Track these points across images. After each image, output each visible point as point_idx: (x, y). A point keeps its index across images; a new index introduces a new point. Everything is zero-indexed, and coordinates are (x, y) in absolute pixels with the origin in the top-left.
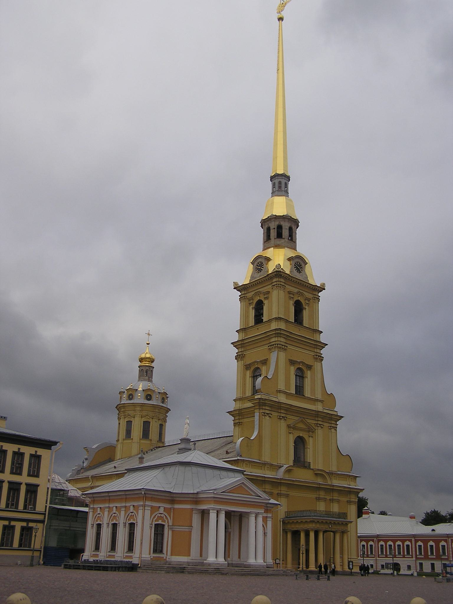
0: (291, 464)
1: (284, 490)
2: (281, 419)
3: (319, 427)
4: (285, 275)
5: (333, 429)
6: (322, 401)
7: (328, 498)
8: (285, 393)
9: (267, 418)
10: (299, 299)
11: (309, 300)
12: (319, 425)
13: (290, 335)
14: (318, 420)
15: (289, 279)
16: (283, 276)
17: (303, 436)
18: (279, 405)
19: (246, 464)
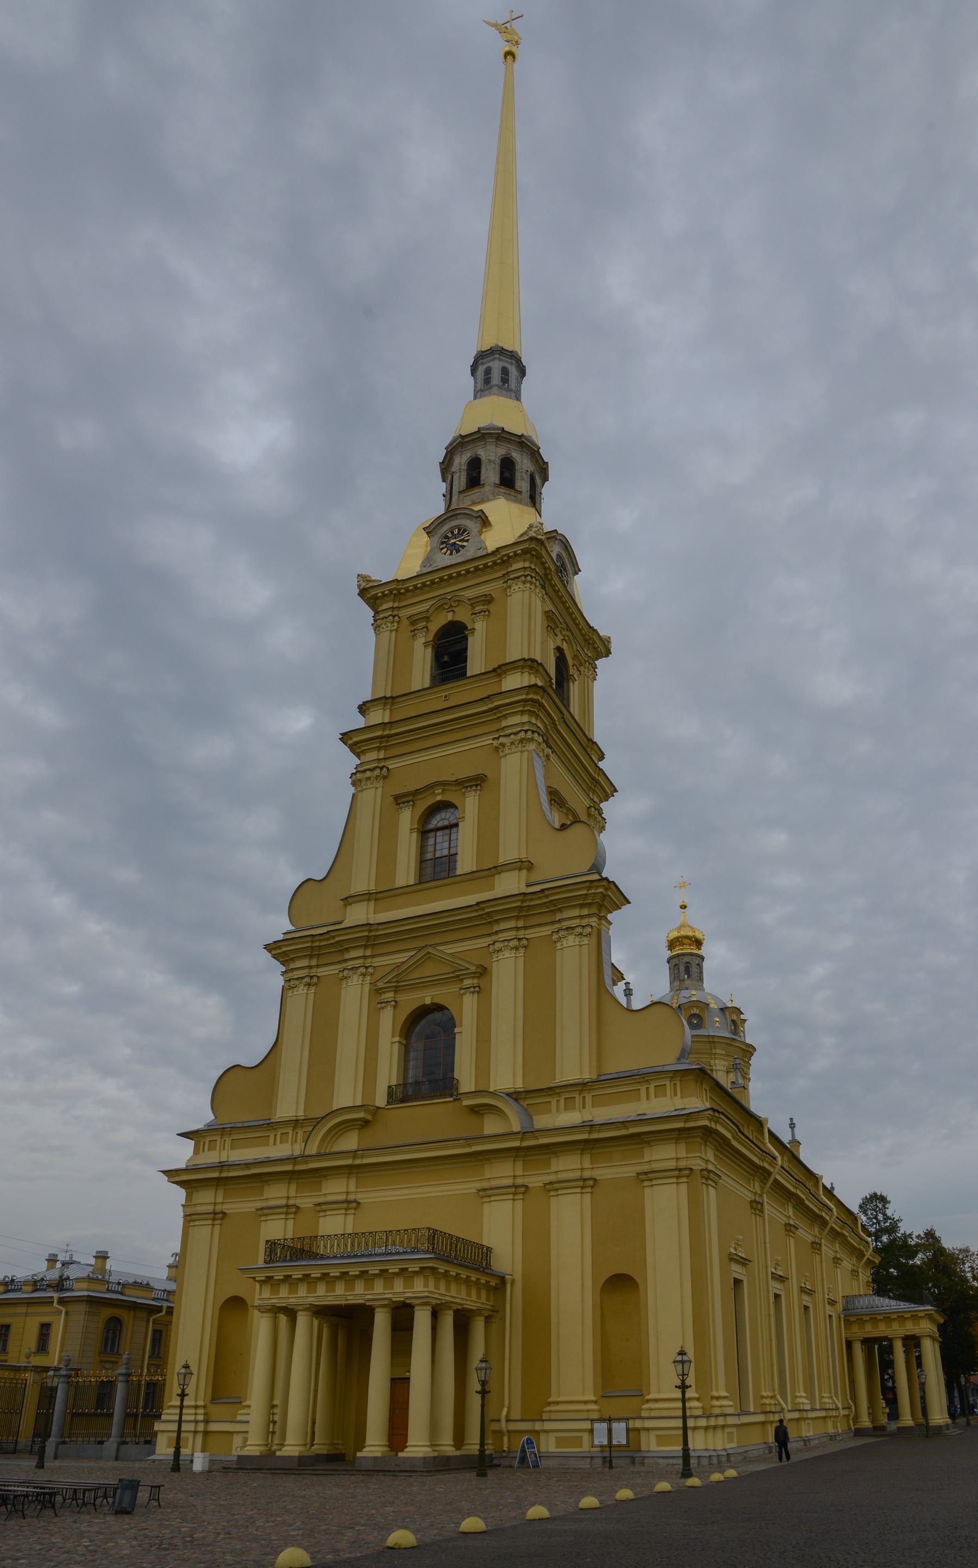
0: (381, 1100)
1: (335, 1189)
2: (345, 978)
3: (501, 950)
4: (386, 590)
5: (571, 938)
6: (525, 865)
7: (535, 1181)
8: (369, 900)
9: (301, 990)
10: (450, 617)
11: (488, 600)
12: (497, 946)
13: (387, 733)
14: (497, 933)
15: (407, 590)
16: (379, 595)
17: (433, 1002)
18: (332, 941)
19: (210, 1141)
